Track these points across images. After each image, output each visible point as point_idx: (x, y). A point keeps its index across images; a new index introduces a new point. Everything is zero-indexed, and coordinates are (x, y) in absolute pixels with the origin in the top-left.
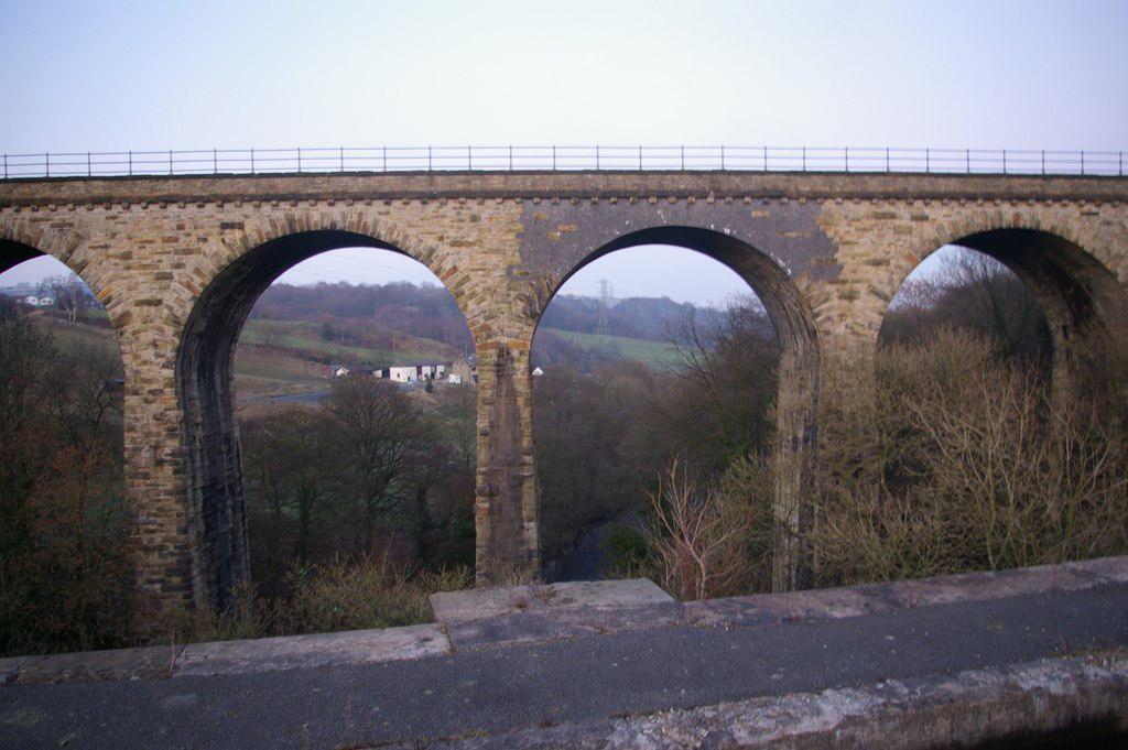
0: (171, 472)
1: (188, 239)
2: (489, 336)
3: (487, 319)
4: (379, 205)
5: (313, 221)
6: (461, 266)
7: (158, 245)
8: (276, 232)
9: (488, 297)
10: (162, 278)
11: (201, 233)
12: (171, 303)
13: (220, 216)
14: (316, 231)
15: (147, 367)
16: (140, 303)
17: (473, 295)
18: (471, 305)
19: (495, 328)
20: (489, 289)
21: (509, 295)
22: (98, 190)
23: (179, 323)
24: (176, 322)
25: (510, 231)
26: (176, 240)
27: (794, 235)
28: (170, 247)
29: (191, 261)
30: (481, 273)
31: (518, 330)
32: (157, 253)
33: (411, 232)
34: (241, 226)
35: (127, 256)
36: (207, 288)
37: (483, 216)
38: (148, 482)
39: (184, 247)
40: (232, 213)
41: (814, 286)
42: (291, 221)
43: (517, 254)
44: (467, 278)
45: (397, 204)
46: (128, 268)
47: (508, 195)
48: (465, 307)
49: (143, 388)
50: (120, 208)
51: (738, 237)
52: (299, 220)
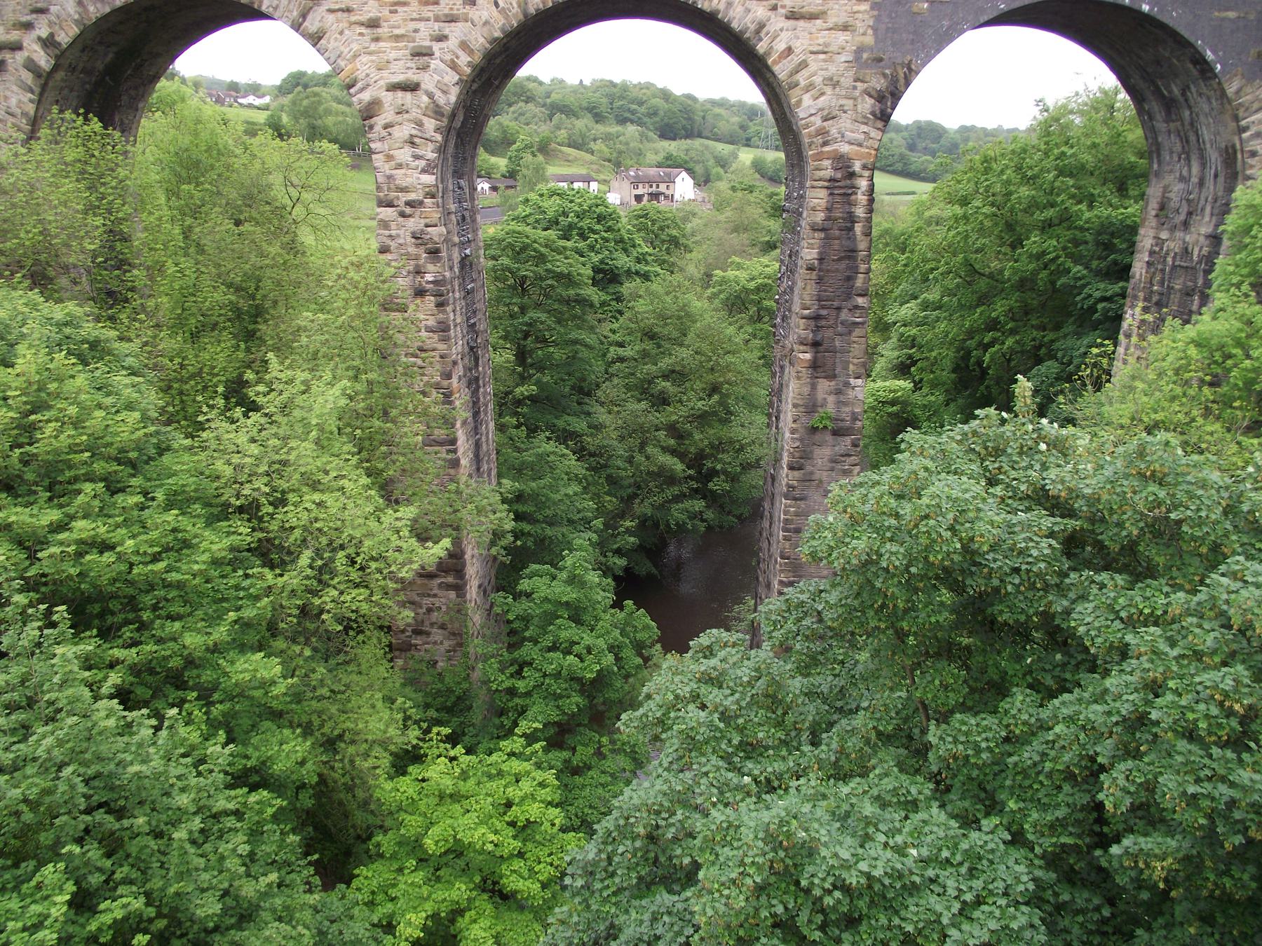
2: (825, 144)
6: (800, 45)
9: (829, 90)
12: (431, 88)
15: (403, 171)
16: (394, 87)
18: (807, 100)
19: (834, 131)
20: (831, 79)
21: (855, 88)
23: (443, 115)
24: (437, 112)
27: (1231, 14)
29: (456, 32)
30: (822, 56)
31: (862, 136)
32: (412, 20)
35: (373, 24)
36: (474, 68)
39: (446, 11)
41: (1248, 89)
43: (870, 32)
44: (803, 65)
46: (377, 40)
48: (799, 103)
49: (398, 198)
51: (1159, 17)
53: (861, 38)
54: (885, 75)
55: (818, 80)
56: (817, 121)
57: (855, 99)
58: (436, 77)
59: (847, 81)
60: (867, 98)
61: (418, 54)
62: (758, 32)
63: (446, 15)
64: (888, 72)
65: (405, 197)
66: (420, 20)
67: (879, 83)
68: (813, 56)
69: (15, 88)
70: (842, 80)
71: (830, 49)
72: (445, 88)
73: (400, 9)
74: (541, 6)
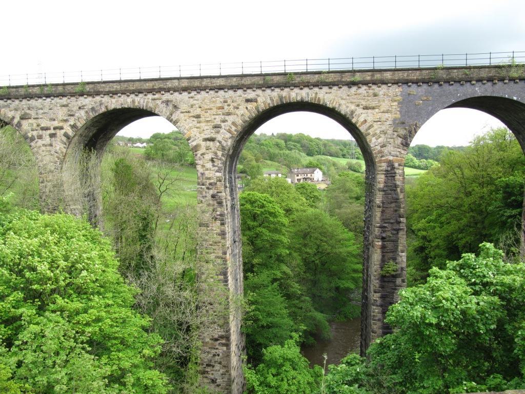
0: (219, 224)
1: (229, 108)
2: (382, 157)
3: (382, 147)
4: (325, 89)
6: (370, 119)
7: (214, 111)
8: (273, 104)
11: (235, 104)
12: (220, 139)
13: (246, 96)
14: (294, 102)
15: (209, 172)
16: (206, 140)
18: (374, 140)
19: (386, 151)
20: (383, 131)
21: (394, 134)
22: (185, 84)
24: (223, 149)
25: (395, 101)
26: (223, 108)
28: (220, 112)
29: (230, 119)
30: (379, 123)
32: (213, 115)
33: (343, 102)
35: (198, 117)
38: (208, 228)
39: (227, 111)
40: (251, 94)
42: (281, 98)
44: (371, 127)
45: (335, 88)
46: (199, 122)
47: (396, 83)
48: (371, 141)
50: (195, 93)
51: (522, 102)
54: (405, 129)
55: (378, 132)
56: (378, 148)
57: (394, 139)
58: (223, 136)
59: (390, 132)
60: (399, 138)
61: (217, 127)
64: (407, 127)
65: (208, 182)
66: (217, 115)
67: (402, 132)
68: (375, 123)
69: (59, 143)
70: (388, 131)
71: (382, 120)
74: (264, 108)
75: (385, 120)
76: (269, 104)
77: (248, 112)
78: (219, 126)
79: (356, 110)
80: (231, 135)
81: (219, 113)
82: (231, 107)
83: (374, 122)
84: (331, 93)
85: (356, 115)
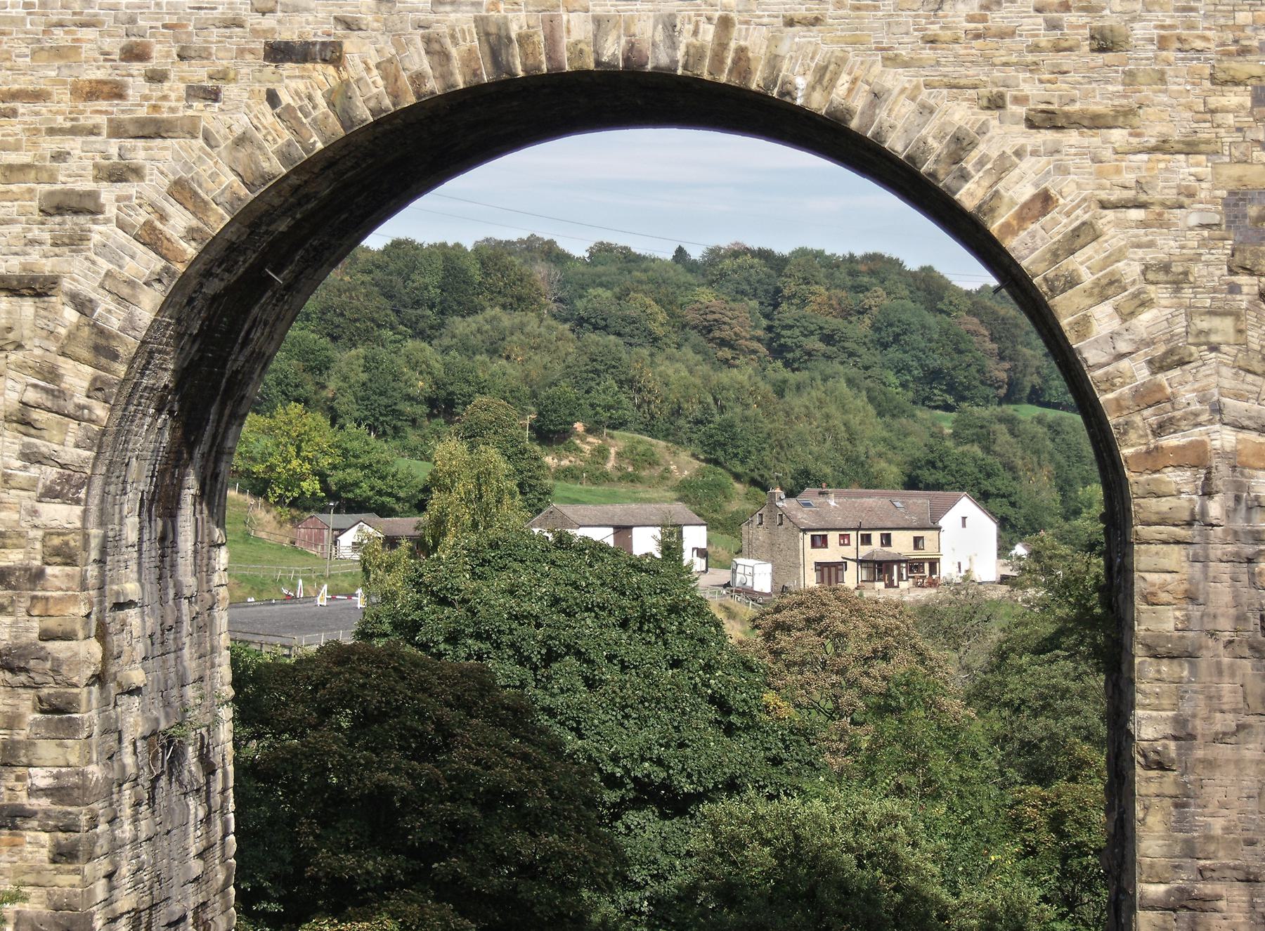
0: (44, 854)
1: (156, 90)
2: (1160, 429)
3: (1158, 365)
5: (565, 41)
6: (1069, 191)
7: (61, 107)
8: (445, 76)
9: (1160, 294)
10: (60, 210)
11: (199, 73)
12: (88, 288)
14: (580, 76)
17: (1107, 287)
18: (1104, 318)
19: (1187, 396)
20: (1166, 268)
21: (1234, 289)
24: (103, 348)
26: (117, 92)
28: (97, 113)
32: (52, 131)
33: (895, 80)
34: (332, 54)
37: (1140, 31)
39: (142, 113)
44: (1082, 235)
48: (1084, 324)
52: (524, 40)
53: (1237, 170)
55: (1130, 269)
57: (1236, 315)
58: (104, 265)
62: (955, 157)
63: (141, 123)
66: (74, 131)
68: (1110, 214)
70: (1197, 270)
71: (1155, 196)
72: (125, 291)
73: (21, 107)
74: (387, 102)
75: (1171, 195)
76: (418, 78)
77: (280, 126)
78: (91, 206)
79: (982, 130)
80: (158, 264)
81: (88, 120)
82: (174, 88)
83: (1104, 205)
84: (816, 21)
85: (981, 163)
